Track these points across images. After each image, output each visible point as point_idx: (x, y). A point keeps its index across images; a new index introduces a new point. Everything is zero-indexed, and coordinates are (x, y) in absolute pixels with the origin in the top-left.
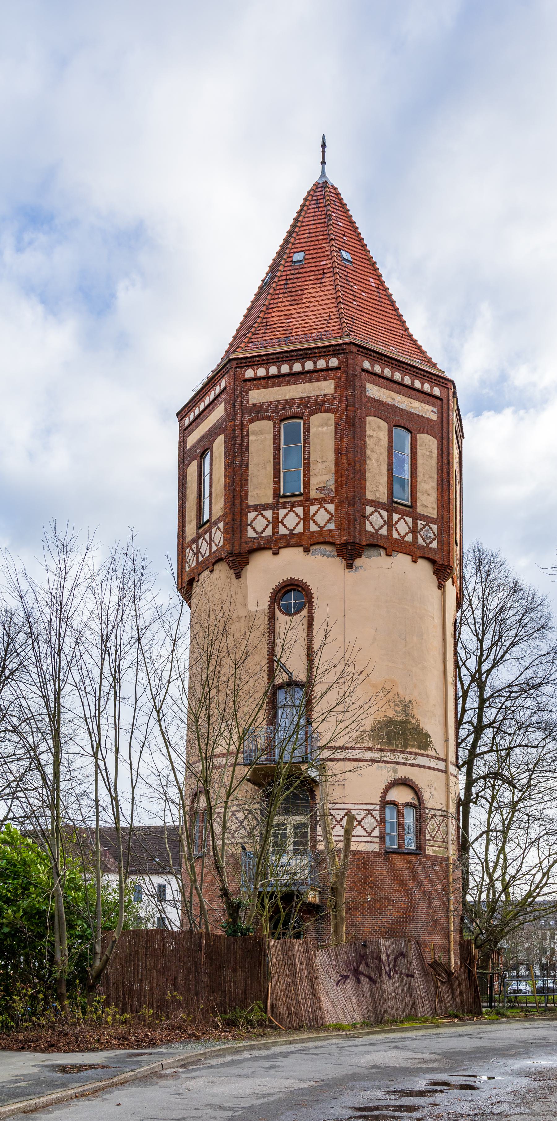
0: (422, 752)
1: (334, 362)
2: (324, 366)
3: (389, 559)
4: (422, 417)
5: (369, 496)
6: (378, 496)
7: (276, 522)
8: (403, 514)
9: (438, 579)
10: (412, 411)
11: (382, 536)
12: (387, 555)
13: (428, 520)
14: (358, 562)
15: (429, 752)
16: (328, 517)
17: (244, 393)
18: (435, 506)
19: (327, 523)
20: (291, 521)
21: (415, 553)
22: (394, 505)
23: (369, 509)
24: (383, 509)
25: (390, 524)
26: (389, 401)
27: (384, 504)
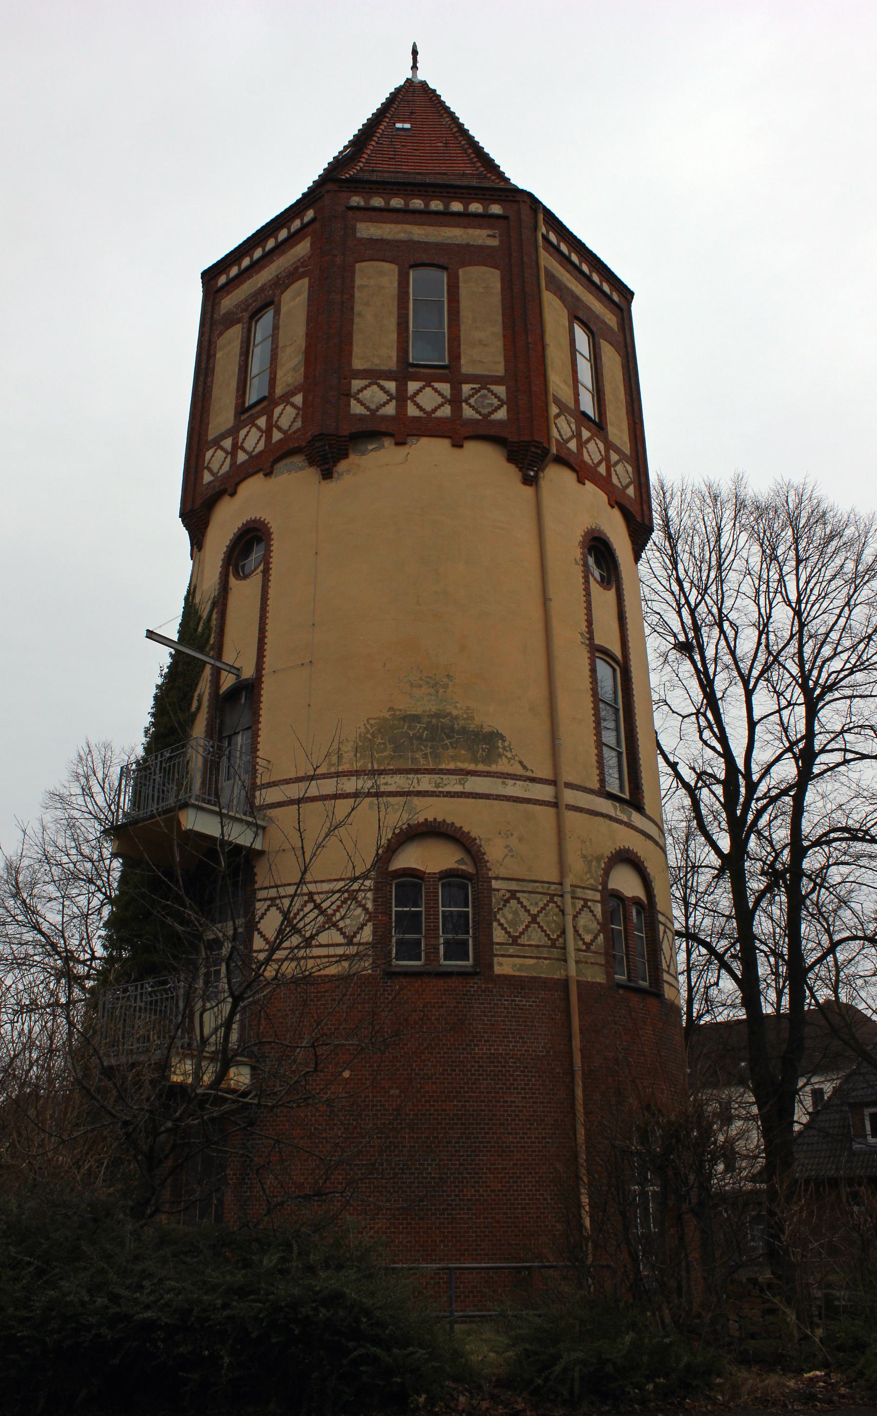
0: (481, 767)
3: (403, 451)
4: (468, 246)
5: (358, 364)
6: (378, 362)
8: (428, 381)
9: (521, 469)
10: (449, 241)
11: (385, 418)
12: (397, 444)
13: (484, 381)
14: (342, 466)
15: (502, 766)
18: (501, 359)
19: (292, 423)
21: (457, 433)
22: (411, 370)
26: (402, 236)
27: (390, 372)
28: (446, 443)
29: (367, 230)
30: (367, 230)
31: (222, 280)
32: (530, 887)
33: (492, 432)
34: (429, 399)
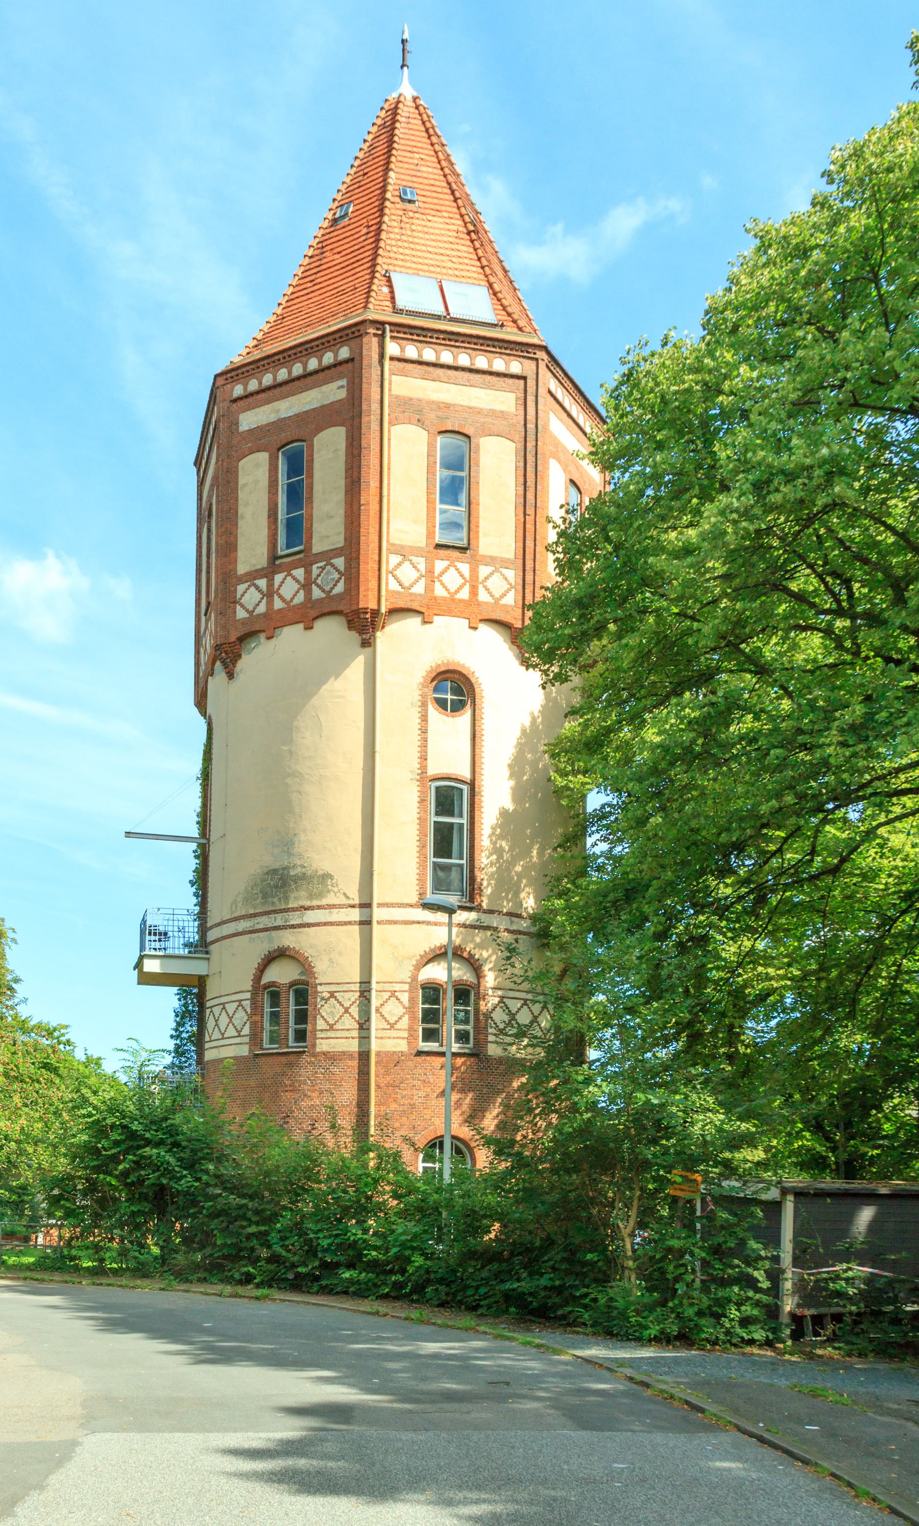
2: (332, 361)
32: (345, 987)
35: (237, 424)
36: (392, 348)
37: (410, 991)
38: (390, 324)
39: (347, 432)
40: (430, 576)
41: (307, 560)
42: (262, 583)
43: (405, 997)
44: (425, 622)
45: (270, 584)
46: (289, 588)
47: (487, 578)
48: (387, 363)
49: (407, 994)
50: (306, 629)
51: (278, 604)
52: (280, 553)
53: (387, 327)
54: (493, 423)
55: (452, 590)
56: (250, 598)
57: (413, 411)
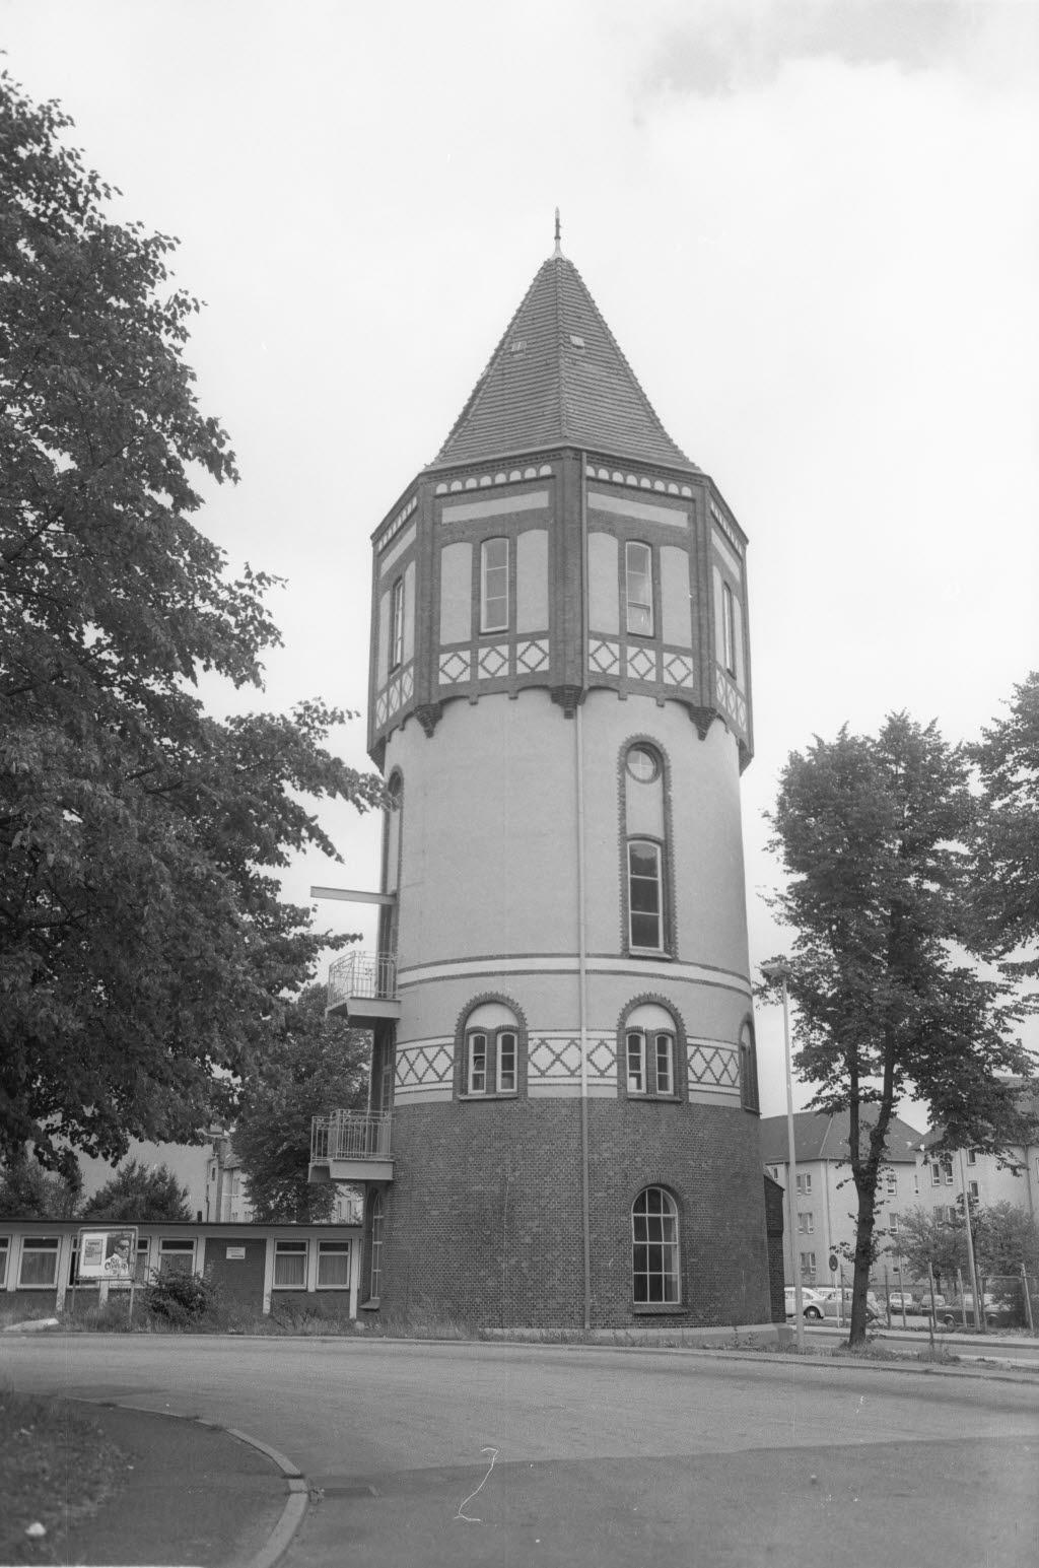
1: (546, 470)
7: (475, 664)
16: (540, 655)
17: (437, 515)
20: (494, 662)
23: (593, 644)
24: (612, 641)
25: (622, 658)
28: (652, 701)
29: (597, 501)
30: (597, 501)
31: (442, 489)
33: (686, 698)
34: (641, 664)
35: (440, 515)
36: (590, 471)
37: (618, 1040)
38: (587, 451)
39: (550, 534)
40: (622, 658)
41: (511, 637)
42: (466, 655)
43: (613, 1045)
44: (620, 699)
45: (474, 656)
46: (494, 662)
47: (669, 665)
48: (584, 483)
49: (615, 1043)
50: (511, 698)
51: (482, 674)
52: (484, 630)
53: (585, 454)
54: (671, 536)
55: (642, 672)
56: (453, 669)
57: (608, 523)
